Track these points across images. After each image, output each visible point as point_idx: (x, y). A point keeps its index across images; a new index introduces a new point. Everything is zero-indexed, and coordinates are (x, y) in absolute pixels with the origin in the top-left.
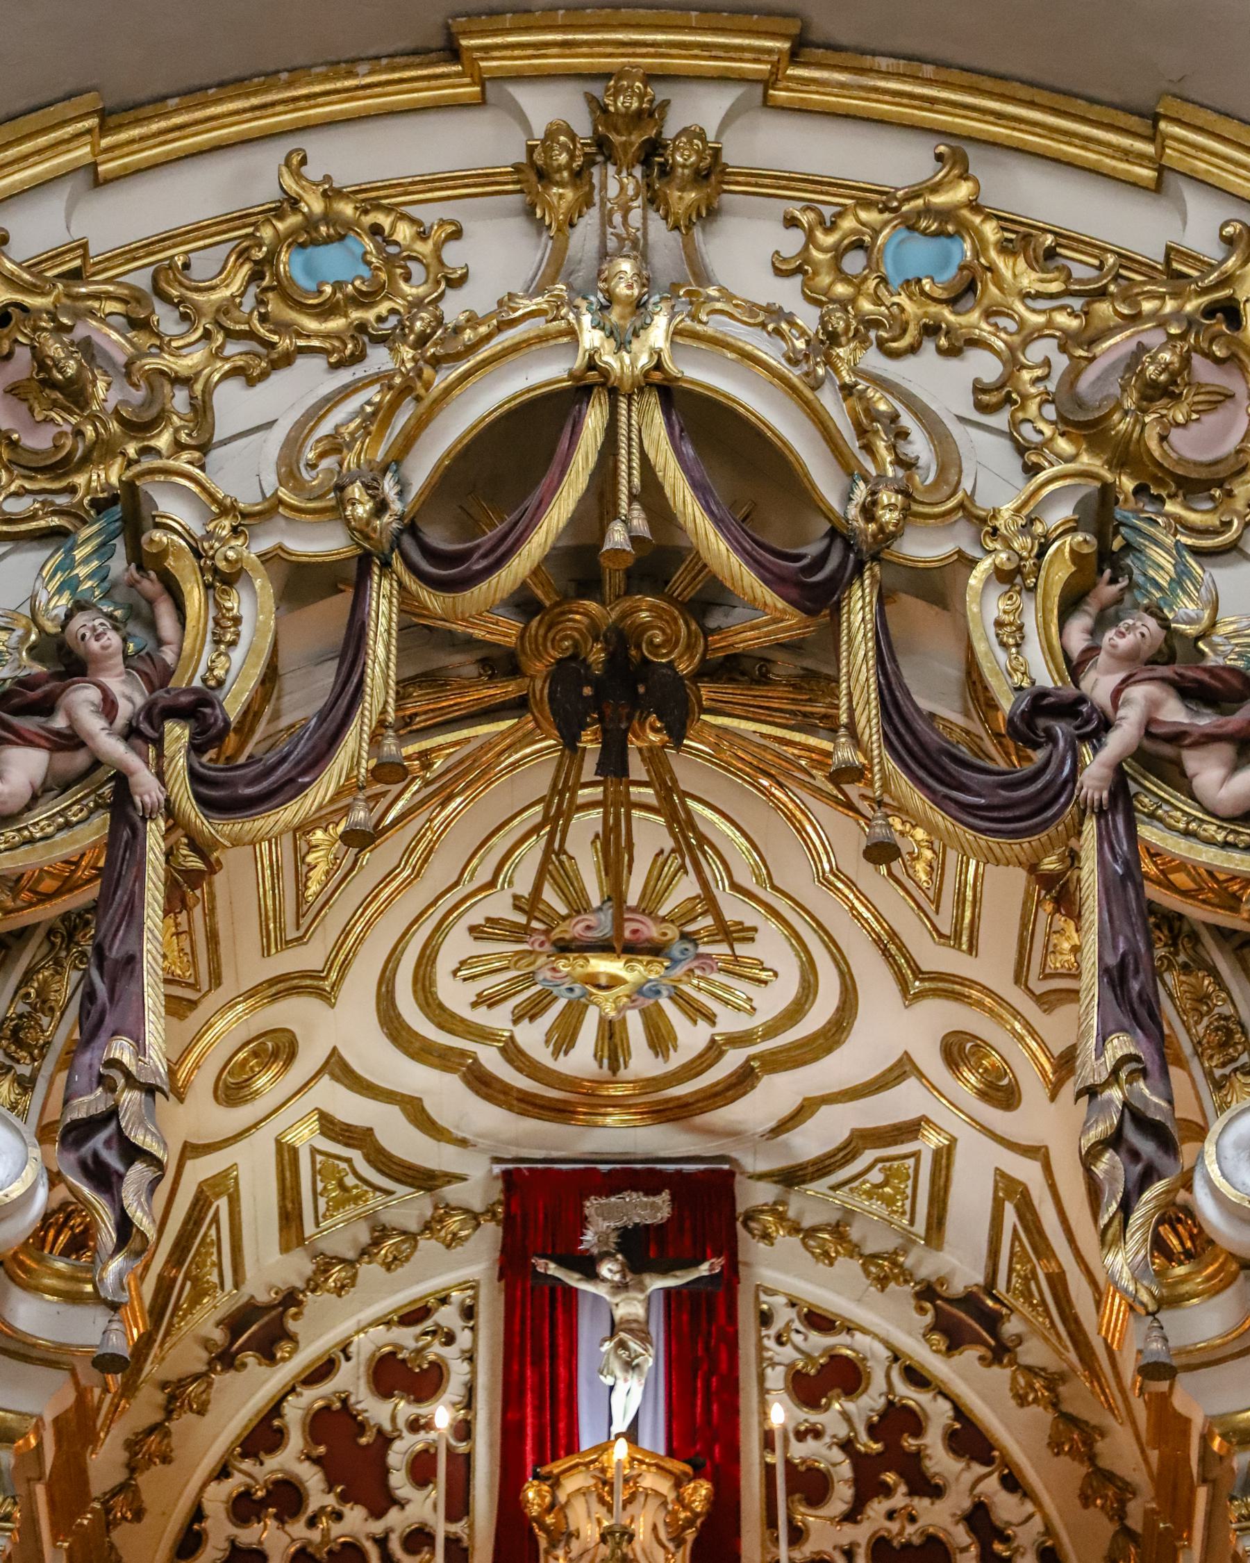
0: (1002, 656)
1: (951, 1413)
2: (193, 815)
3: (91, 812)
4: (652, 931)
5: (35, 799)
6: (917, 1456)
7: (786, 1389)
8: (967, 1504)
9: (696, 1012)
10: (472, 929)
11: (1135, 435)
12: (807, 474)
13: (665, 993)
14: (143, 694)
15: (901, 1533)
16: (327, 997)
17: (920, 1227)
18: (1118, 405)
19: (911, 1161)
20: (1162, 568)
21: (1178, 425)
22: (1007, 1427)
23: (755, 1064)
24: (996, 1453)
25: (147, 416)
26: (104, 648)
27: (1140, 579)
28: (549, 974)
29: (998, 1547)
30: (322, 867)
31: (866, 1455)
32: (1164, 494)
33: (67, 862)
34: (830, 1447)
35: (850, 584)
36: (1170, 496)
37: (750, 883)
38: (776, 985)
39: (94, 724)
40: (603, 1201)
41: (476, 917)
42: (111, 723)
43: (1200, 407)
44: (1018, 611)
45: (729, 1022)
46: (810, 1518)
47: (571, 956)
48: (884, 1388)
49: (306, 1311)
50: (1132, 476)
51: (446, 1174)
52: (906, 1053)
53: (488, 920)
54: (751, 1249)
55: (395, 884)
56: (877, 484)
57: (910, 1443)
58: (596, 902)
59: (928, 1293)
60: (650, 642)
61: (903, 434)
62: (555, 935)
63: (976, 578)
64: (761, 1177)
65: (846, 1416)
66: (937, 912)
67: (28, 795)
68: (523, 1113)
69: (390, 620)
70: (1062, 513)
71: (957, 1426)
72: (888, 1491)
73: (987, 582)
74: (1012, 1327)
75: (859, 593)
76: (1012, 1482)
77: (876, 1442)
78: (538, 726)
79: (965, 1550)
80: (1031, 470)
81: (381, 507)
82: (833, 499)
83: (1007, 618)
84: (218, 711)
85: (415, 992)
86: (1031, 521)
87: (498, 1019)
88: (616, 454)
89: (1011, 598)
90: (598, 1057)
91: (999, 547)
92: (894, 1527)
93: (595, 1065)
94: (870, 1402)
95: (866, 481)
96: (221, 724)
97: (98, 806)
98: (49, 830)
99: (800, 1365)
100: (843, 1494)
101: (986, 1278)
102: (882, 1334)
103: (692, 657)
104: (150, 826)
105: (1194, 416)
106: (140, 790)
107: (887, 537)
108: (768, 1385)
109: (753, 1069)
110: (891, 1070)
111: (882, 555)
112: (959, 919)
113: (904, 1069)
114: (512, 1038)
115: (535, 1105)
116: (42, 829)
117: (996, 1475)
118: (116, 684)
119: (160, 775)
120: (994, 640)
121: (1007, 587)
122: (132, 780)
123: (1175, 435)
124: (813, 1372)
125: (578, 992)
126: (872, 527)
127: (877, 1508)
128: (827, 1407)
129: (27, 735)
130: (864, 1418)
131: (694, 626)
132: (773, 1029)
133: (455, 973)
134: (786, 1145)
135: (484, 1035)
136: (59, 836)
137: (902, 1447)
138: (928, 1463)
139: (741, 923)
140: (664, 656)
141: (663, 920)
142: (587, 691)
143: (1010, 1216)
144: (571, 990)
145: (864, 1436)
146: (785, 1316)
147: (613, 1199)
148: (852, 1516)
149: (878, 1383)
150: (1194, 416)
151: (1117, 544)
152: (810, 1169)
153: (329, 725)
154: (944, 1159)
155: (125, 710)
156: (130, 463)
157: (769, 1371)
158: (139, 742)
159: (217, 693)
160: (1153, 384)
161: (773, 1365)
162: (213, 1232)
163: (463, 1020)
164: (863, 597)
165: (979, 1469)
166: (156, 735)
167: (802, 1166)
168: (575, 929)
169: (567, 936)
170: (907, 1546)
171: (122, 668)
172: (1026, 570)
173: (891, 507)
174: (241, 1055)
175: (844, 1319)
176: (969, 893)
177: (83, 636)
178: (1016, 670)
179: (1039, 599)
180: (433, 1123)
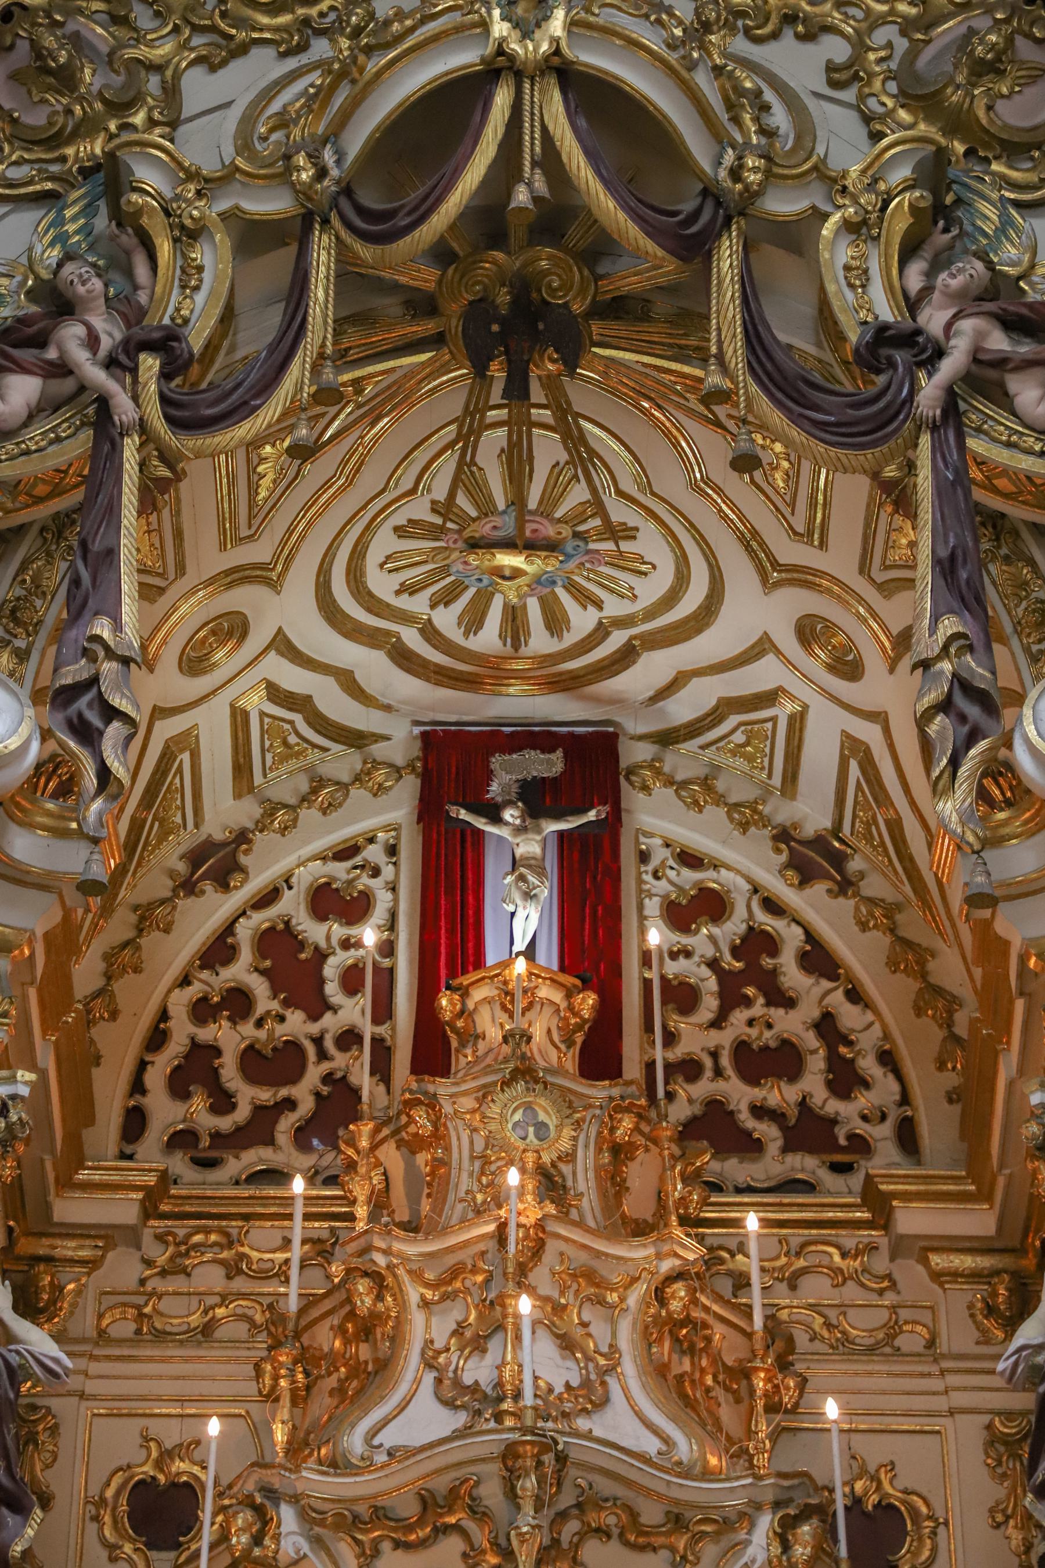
0: (849, 295)
1: (803, 937)
2: (162, 432)
3: (77, 429)
4: (549, 531)
5: (31, 418)
6: (774, 972)
7: (661, 916)
8: (816, 1013)
9: (586, 599)
10: (396, 529)
11: (966, 106)
12: (683, 143)
13: (560, 583)
14: (119, 327)
15: (759, 1038)
16: (275, 585)
17: (777, 780)
18: (951, 81)
19: (769, 725)
20: (988, 219)
21: (1003, 96)
22: (851, 948)
23: (636, 643)
24: (841, 971)
25: (126, 98)
26: (88, 291)
27: (968, 228)
28: (461, 567)
29: (843, 1050)
30: (270, 476)
31: (730, 972)
32: (990, 156)
33: (58, 471)
34: (699, 965)
35: (719, 236)
36: (996, 158)
37: (632, 490)
38: (654, 576)
39: (80, 356)
40: (507, 757)
41: (400, 519)
42: (95, 354)
43: (1022, 81)
44: (864, 257)
45: (614, 607)
46: (682, 1025)
47: (480, 551)
48: (746, 915)
50: (963, 141)
51: (374, 735)
52: (765, 633)
53: (410, 521)
54: (634, 801)
55: (331, 491)
56: (743, 150)
57: (767, 962)
58: (501, 505)
59: (783, 836)
60: (549, 286)
61: (766, 108)
62: (467, 533)
63: (827, 230)
64: (641, 738)
65: (711, 938)
66: (793, 514)
67: (24, 414)
68: (438, 684)
69: (328, 268)
70: (903, 173)
71: (808, 948)
72: (748, 1002)
73: (837, 233)
74: (855, 864)
75: (728, 243)
76: (855, 995)
77: (738, 961)
78: (454, 357)
79: (814, 1052)
80: (876, 137)
82: (706, 165)
83: (854, 263)
84: (184, 345)
85: (348, 582)
86: (876, 181)
87: (418, 604)
88: (521, 127)
89: (857, 246)
91: (847, 202)
92: (754, 1032)
93: (499, 643)
94: (733, 927)
95: (734, 148)
96: (186, 355)
97: (83, 424)
98: (43, 443)
99: (673, 896)
100: (710, 1005)
101: (833, 823)
102: (745, 871)
103: (584, 299)
104: (127, 441)
105: (1017, 89)
106: (118, 411)
107: (752, 195)
108: (647, 912)
109: (634, 646)
110: (753, 647)
111: (748, 211)
112: (812, 519)
113: (763, 647)
114: (429, 620)
115: (450, 677)
116: (37, 443)
118: (99, 323)
119: (135, 398)
120: (843, 282)
121: (854, 237)
122: (112, 402)
123: (1000, 106)
124: (684, 902)
125: (486, 582)
126: (739, 187)
127: (739, 1017)
128: (697, 931)
129: (25, 365)
130: (728, 940)
131: (586, 272)
132: (651, 613)
133: (382, 566)
134: (662, 712)
135: (406, 618)
136: (50, 449)
137: (761, 966)
138: (782, 979)
139: (625, 524)
140: (560, 298)
141: (559, 521)
143: (854, 770)
144: (480, 580)
145: (728, 956)
146: (660, 855)
147: (514, 756)
148: (717, 1023)
149: (740, 911)
150: (1017, 89)
151: (949, 199)
152: (682, 732)
153: (278, 357)
154: (797, 723)
155: (106, 344)
156: (111, 137)
157: (647, 901)
158: (118, 372)
159: (183, 330)
160: (982, 61)
161: (651, 896)
163: (388, 605)
164: (731, 247)
165: (826, 984)
166: (132, 365)
167: (676, 729)
168: (484, 529)
169: (477, 535)
170: (766, 1048)
171: (104, 308)
172: (871, 222)
173: (755, 170)
174: (202, 634)
176: (820, 497)
177: (72, 282)
178: (861, 307)
179: (882, 247)
180: (362, 691)
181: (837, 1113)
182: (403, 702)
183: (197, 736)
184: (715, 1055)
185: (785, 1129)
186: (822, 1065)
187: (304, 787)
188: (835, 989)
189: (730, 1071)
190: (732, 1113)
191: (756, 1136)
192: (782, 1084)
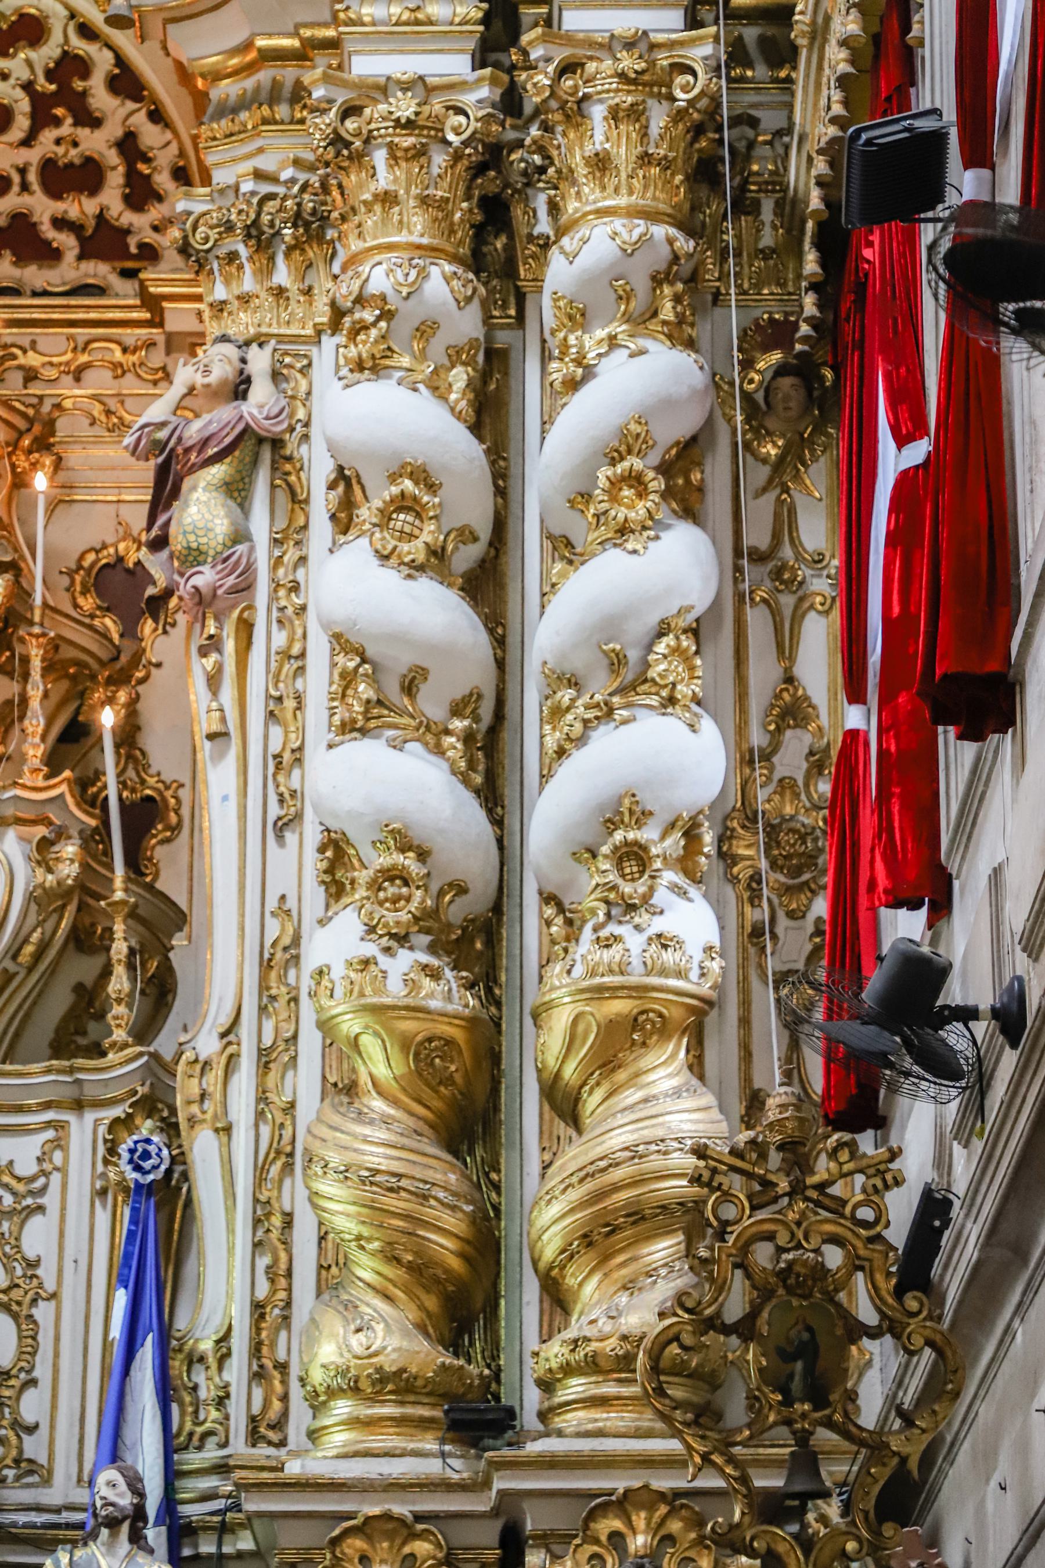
1: (113, 61)
6: (84, 94)
8: (119, 133)
15: (65, 155)
22: (154, 71)
24: (145, 93)
29: (141, 167)
31: (43, 94)
34: (14, 87)
48: (61, 40)
57: (79, 85)
65: (29, 63)
71: (117, 71)
72: (57, 122)
76: (157, 116)
77: (51, 83)
79: (114, 168)
92: (60, 150)
94: (48, 53)
100: (22, 124)
117: (143, 112)
127: (48, 136)
130: (43, 64)
137: (72, 89)
138: (91, 100)
145: (41, 79)
148: (27, 142)
149: (56, 37)
165: (131, 105)
170: (70, 165)
181: (131, 224)
184: (22, 171)
185: (83, 241)
186: (121, 180)
188: (138, 110)
189: (36, 187)
190: (35, 225)
191: (55, 245)
192: (83, 199)
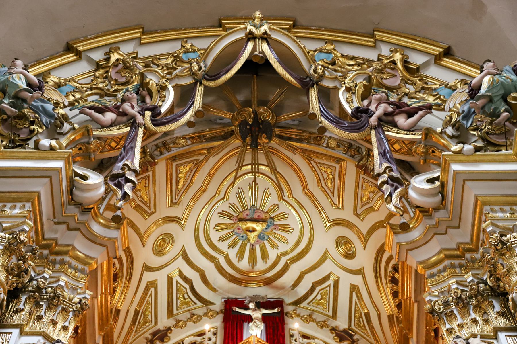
4: (263, 216)
17: (330, 314)
19: (328, 288)
23: (288, 262)
49: (173, 332)
59: (333, 329)
62: (239, 217)
64: (290, 304)
81: (200, 68)
90: (249, 262)
93: (247, 264)
101: (348, 326)
102: (322, 339)
114: (228, 254)
126: (316, 75)
133: (214, 228)
141: (266, 212)
142: (248, 127)
144: (242, 237)
146: (297, 336)
154: (336, 283)
162: (150, 299)
167: (300, 298)
168: (244, 215)
169: (242, 217)
173: (321, 69)
175: (312, 336)
182: (219, 288)
183: (157, 283)
187: (189, 316)
